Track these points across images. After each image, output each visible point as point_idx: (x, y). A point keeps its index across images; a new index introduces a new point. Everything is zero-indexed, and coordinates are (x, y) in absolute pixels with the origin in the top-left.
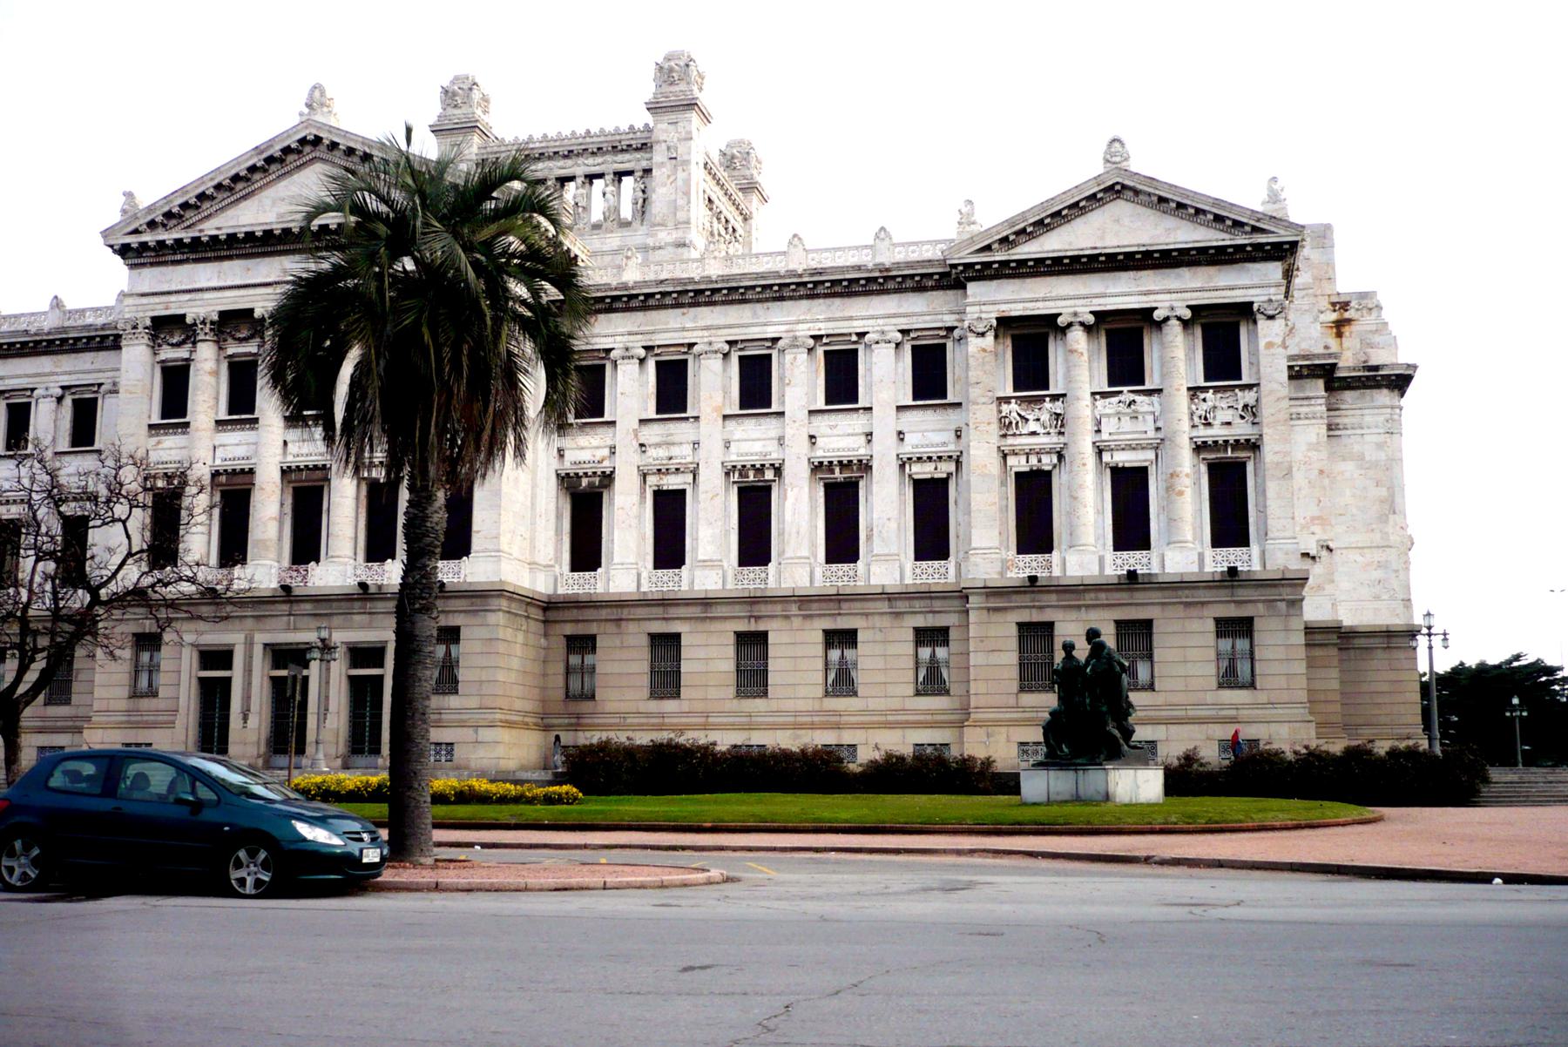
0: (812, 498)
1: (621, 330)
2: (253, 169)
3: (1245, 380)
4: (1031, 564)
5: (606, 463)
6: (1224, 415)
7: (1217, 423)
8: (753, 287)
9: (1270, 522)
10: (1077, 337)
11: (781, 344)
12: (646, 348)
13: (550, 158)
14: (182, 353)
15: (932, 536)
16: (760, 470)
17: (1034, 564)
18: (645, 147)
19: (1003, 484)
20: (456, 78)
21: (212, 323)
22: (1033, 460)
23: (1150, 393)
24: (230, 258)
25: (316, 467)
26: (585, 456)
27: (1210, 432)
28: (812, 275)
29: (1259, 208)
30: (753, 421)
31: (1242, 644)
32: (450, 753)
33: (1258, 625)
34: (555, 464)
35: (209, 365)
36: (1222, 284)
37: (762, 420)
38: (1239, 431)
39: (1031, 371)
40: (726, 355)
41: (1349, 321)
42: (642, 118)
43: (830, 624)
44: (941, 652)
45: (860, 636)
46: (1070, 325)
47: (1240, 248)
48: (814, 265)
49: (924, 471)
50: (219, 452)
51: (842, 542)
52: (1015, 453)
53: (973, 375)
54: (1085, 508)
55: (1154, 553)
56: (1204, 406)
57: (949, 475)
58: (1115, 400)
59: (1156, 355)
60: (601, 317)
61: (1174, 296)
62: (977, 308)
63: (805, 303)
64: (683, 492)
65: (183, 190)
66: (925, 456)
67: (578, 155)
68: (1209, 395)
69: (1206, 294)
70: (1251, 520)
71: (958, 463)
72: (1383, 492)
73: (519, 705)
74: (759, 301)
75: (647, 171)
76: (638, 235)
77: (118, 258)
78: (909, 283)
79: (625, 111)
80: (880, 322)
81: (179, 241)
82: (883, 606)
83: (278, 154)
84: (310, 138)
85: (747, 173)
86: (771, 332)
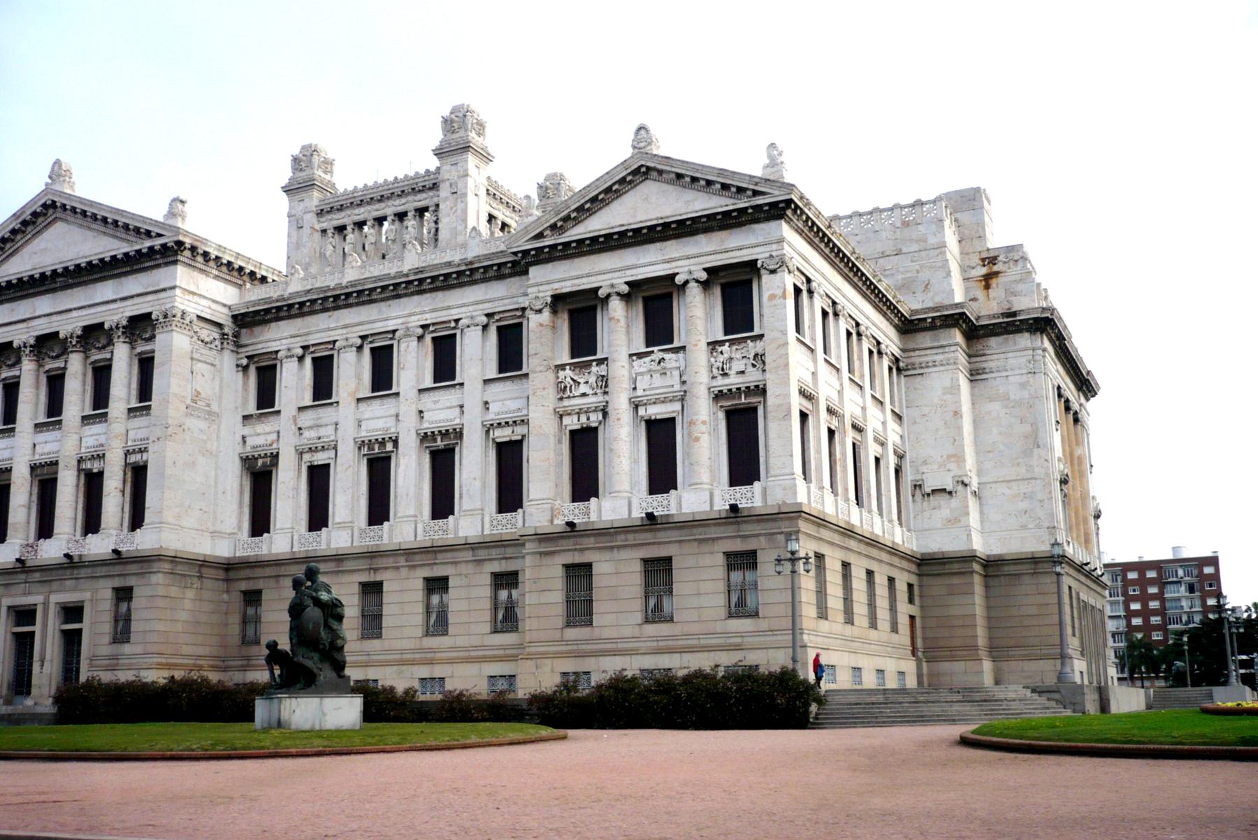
1: (285, 334)
3: (757, 331)
6: (738, 365)
7: (732, 372)
10: (616, 306)
11: (397, 334)
13: (368, 203)
16: (382, 443)
17: (577, 511)
20: (303, 148)
26: (260, 441)
27: (727, 381)
28: (416, 273)
34: (239, 449)
37: (386, 401)
38: (751, 379)
39: (584, 342)
41: (997, 274)
42: (433, 163)
46: (609, 296)
47: (742, 211)
54: (624, 457)
56: (721, 358)
58: (647, 359)
61: (692, 261)
63: (416, 298)
64: (328, 465)
66: (503, 422)
67: (388, 198)
68: (726, 348)
70: (762, 460)
72: (1027, 428)
73: (186, 650)
74: (383, 300)
80: (471, 308)
82: (468, 555)
83: (29, 218)
84: (49, 202)
86: (391, 325)
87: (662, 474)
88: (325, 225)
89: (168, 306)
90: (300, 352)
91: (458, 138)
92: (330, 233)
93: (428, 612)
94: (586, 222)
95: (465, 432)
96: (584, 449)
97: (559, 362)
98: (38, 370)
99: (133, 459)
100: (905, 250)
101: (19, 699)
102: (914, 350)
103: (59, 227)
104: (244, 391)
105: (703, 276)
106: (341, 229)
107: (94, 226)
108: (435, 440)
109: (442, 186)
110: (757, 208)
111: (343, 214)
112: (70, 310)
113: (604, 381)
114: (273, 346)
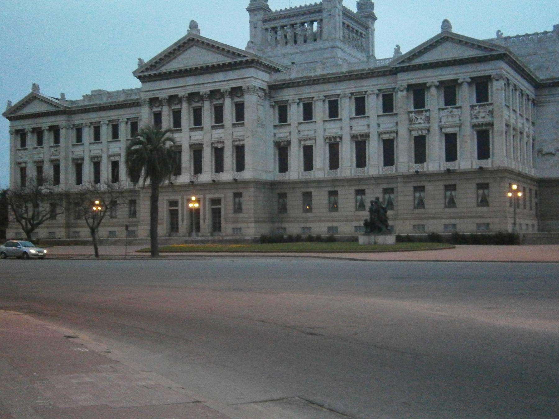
0: (351, 147)
2: (175, 50)
3: (490, 102)
5: (288, 138)
6: (482, 115)
7: (480, 117)
10: (433, 90)
11: (341, 96)
12: (299, 99)
15: (389, 158)
16: (335, 138)
19: (410, 140)
22: (420, 132)
23: (457, 108)
24: (171, 78)
26: (282, 135)
33: (491, 185)
37: (335, 121)
39: (419, 103)
40: (324, 101)
43: (357, 188)
49: (386, 137)
52: (413, 130)
54: (436, 148)
56: (475, 112)
57: (394, 138)
58: (446, 111)
60: (285, 89)
61: (465, 74)
68: (477, 108)
70: (491, 150)
75: (321, 20)
76: (319, 44)
81: (155, 74)
82: (373, 181)
86: (338, 92)
87: (451, 154)
88: (267, 27)
89: (249, 84)
90: (298, 101)
93: (356, 202)
95: (371, 135)
97: (410, 110)
98: (189, 107)
99: (237, 143)
100: (539, 53)
101: (216, 233)
102: (541, 95)
103: (194, 47)
104: (273, 116)
105: (469, 80)
106: (274, 29)
107: (212, 49)
108: (357, 138)
109: (324, 11)
110: (492, 56)
111: (276, 22)
112: (203, 84)
113: (428, 119)
114: (287, 98)
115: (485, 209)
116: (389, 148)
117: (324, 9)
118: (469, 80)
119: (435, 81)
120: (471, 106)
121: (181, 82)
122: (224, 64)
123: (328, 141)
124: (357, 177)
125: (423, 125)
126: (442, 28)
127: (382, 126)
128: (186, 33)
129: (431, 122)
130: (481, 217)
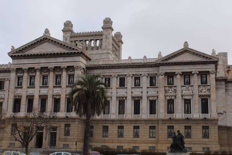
2: (35, 43)
4: (170, 116)
6: (204, 91)
8: (122, 66)
9: (212, 109)
10: (178, 76)
11: (127, 76)
13: (84, 37)
14: (22, 75)
15: (153, 110)
16: (123, 98)
17: (170, 116)
18: (101, 35)
19: (165, 101)
21: (27, 70)
22: (171, 97)
23: (191, 86)
24: (31, 58)
25: (45, 95)
27: (202, 93)
29: (211, 55)
30: (122, 89)
31: (207, 131)
32: (68, 146)
33: (210, 127)
35: (26, 77)
36: (204, 68)
37: (123, 89)
40: (117, 77)
41: (230, 70)
43: (134, 125)
44: (154, 131)
45: (140, 127)
46: (177, 74)
48: (133, 62)
49: (151, 99)
50: (28, 92)
51: (137, 111)
52: (167, 96)
53: (161, 82)
54: (179, 105)
55: (191, 115)
56: (201, 89)
57: (156, 99)
58: (185, 87)
59: (192, 80)
61: (196, 70)
62: (161, 71)
63: (131, 69)
65: (22, 46)
66: (152, 96)
67: (89, 36)
68: (202, 87)
69: (201, 69)
71: (158, 97)
73: (80, 138)
75: (102, 40)
76: (100, 51)
77: (10, 58)
78: (149, 66)
79: (98, 28)
81: (21, 55)
82: (144, 122)
85: (119, 38)
86: (125, 73)
88: (72, 40)
91: (108, 24)
92: (73, 42)
94: (173, 59)
95: (143, 97)
96: (170, 102)
98: (40, 75)
103: (47, 43)
108: (135, 98)
110: (211, 62)
111: (77, 38)
112: (51, 63)
113: (175, 90)
115: (206, 140)
116: (153, 105)
117: (104, 34)
118: (198, 73)
119: (180, 72)
120: (198, 86)
121: (37, 61)
122: (64, 53)
123: (118, 99)
124: (135, 119)
125: (173, 94)
126: (184, 46)
127: (149, 93)
128: (42, 35)
129: (177, 92)
130: (205, 144)
